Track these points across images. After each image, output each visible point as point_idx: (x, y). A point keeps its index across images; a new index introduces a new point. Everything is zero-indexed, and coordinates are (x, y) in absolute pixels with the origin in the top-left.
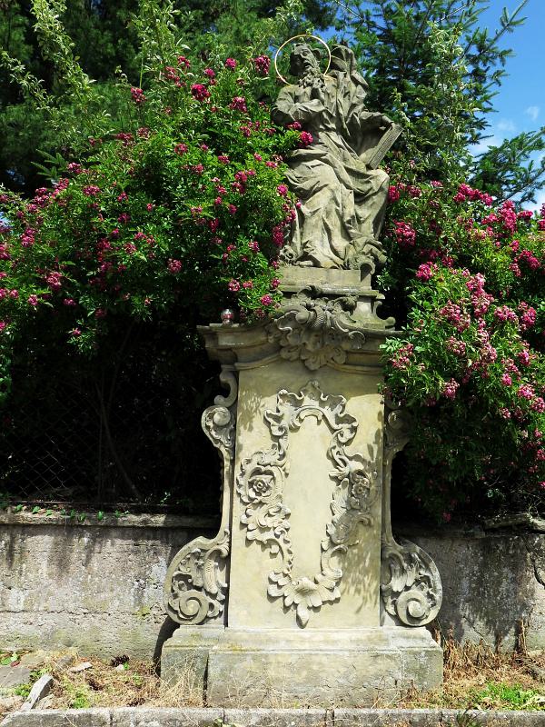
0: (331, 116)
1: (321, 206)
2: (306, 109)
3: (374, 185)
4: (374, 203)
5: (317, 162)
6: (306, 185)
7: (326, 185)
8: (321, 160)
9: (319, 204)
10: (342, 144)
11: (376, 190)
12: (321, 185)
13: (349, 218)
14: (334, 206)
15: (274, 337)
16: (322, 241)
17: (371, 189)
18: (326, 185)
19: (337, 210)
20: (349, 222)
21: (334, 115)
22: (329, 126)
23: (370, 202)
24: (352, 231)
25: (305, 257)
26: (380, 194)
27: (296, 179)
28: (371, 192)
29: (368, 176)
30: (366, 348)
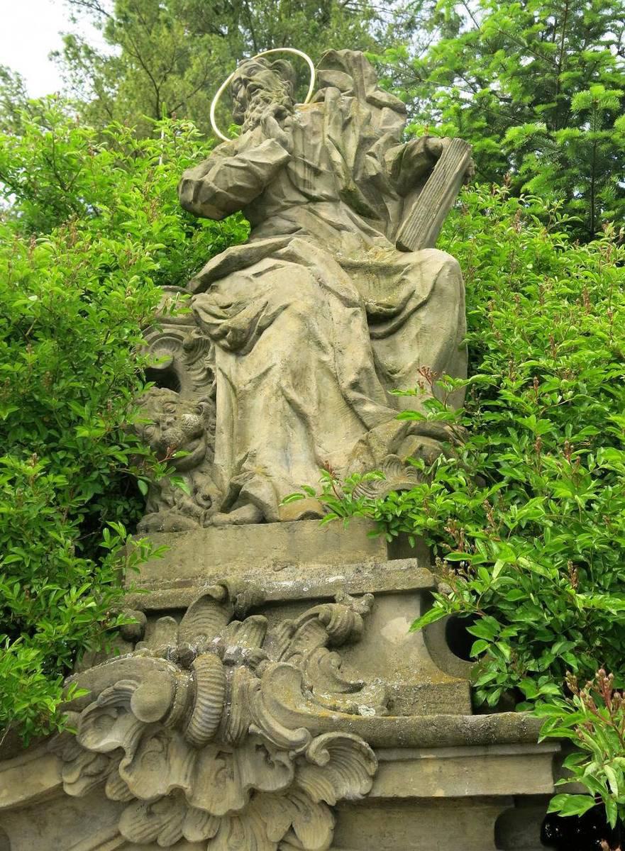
0: (317, 173)
1: (277, 360)
2: (243, 161)
3: (418, 284)
4: (424, 330)
5: (268, 262)
6: (242, 319)
7: (285, 307)
8: (280, 258)
9: (270, 355)
10: (348, 223)
11: (425, 296)
12: (274, 309)
13: (352, 377)
14: (314, 354)
15: (84, 776)
16: (285, 448)
17: (411, 295)
18: (285, 307)
19: (322, 363)
20: (355, 386)
21: (323, 167)
22: (315, 193)
23: (413, 329)
24: (369, 408)
25: (236, 497)
26: (434, 303)
27: (220, 313)
28: (411, 305)
29: (398, 269)
30: (388, 788)
